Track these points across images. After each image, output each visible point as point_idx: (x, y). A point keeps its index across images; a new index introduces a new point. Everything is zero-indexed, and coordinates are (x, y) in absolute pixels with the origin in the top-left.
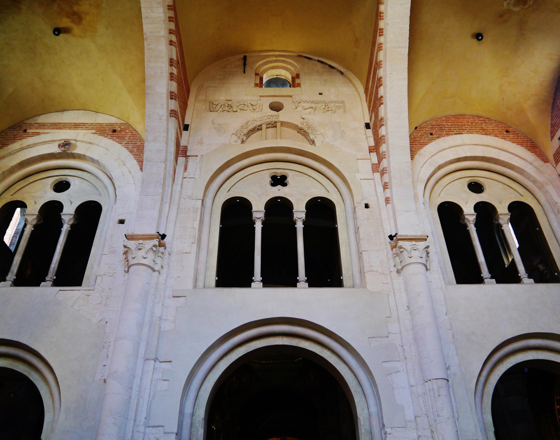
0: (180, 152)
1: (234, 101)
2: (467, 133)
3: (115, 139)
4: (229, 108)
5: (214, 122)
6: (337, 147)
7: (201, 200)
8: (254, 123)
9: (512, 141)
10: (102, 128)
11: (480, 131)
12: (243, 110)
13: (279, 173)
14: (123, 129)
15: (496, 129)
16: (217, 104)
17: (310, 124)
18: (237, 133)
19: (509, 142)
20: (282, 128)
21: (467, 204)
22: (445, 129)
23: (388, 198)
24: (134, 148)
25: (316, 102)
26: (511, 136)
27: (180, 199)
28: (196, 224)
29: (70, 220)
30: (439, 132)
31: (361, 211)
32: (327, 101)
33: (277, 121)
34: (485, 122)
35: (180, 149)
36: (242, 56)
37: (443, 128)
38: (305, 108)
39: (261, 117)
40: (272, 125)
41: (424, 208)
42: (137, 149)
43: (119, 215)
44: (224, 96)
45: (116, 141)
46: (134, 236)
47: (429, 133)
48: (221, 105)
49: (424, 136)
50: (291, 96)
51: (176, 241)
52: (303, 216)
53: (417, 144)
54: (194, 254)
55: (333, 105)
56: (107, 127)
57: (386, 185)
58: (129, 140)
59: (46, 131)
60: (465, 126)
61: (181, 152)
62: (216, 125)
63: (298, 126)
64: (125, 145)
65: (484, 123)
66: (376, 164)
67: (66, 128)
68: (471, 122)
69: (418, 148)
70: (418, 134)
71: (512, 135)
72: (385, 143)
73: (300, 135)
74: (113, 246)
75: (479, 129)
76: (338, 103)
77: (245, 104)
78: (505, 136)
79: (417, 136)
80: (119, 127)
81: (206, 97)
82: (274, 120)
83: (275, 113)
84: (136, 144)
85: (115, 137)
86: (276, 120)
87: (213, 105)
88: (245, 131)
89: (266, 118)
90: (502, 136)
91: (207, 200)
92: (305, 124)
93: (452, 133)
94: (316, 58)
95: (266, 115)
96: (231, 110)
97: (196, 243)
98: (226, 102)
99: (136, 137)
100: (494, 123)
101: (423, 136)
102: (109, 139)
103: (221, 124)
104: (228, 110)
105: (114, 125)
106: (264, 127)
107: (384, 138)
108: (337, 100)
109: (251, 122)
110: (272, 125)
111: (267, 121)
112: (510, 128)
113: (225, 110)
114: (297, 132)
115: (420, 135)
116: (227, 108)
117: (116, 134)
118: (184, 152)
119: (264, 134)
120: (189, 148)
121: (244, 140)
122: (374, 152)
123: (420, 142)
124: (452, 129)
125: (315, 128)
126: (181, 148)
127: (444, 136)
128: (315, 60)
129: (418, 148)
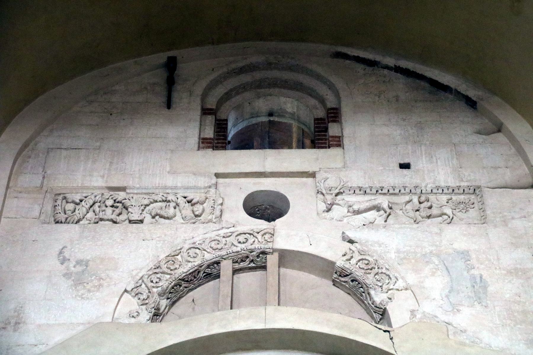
1: (131, 191)
4: (117, 211)
5: (67, 254)
6: (464, 331)
8: (194, 257)
12: (161, 217)
16: (78, 201)
17: (372, 257)
18: (140, 290)
20: (283, 270)
25: (391, 191)
32: (426, 187)
36: (162, 58)
38: (356, 207)
39: (217, 238)
40: (252, 261)
44: (103, 177)
48: (91, 202)
50: (313, 175)
55: (444, 198)
63: (332, 264)
73: (342, 292)
76: (460, 194)
77: (170, 198)
81: (44, 177)
82: (258, 245)
83: (261, 224)
86: (264, 246)
87: (67, 202)
88: (166, 282)
89: (232, 239)
92: (357, 257)
94: (390, 61)
95: (233, 233)
96: (123, 217)
98: (107, 194)
103: (88, 261)
104: (114, 217)
106: (226, 267)
108: (458, 185)
109: (185, 255)
110: (252, 261)
111: (235, 249)
113: (105, 217)
114: (332, 283)
116: (109, 210)
119: (227, 290)
121: (162, 309)
125: (387, 269)
128: (387, 67)
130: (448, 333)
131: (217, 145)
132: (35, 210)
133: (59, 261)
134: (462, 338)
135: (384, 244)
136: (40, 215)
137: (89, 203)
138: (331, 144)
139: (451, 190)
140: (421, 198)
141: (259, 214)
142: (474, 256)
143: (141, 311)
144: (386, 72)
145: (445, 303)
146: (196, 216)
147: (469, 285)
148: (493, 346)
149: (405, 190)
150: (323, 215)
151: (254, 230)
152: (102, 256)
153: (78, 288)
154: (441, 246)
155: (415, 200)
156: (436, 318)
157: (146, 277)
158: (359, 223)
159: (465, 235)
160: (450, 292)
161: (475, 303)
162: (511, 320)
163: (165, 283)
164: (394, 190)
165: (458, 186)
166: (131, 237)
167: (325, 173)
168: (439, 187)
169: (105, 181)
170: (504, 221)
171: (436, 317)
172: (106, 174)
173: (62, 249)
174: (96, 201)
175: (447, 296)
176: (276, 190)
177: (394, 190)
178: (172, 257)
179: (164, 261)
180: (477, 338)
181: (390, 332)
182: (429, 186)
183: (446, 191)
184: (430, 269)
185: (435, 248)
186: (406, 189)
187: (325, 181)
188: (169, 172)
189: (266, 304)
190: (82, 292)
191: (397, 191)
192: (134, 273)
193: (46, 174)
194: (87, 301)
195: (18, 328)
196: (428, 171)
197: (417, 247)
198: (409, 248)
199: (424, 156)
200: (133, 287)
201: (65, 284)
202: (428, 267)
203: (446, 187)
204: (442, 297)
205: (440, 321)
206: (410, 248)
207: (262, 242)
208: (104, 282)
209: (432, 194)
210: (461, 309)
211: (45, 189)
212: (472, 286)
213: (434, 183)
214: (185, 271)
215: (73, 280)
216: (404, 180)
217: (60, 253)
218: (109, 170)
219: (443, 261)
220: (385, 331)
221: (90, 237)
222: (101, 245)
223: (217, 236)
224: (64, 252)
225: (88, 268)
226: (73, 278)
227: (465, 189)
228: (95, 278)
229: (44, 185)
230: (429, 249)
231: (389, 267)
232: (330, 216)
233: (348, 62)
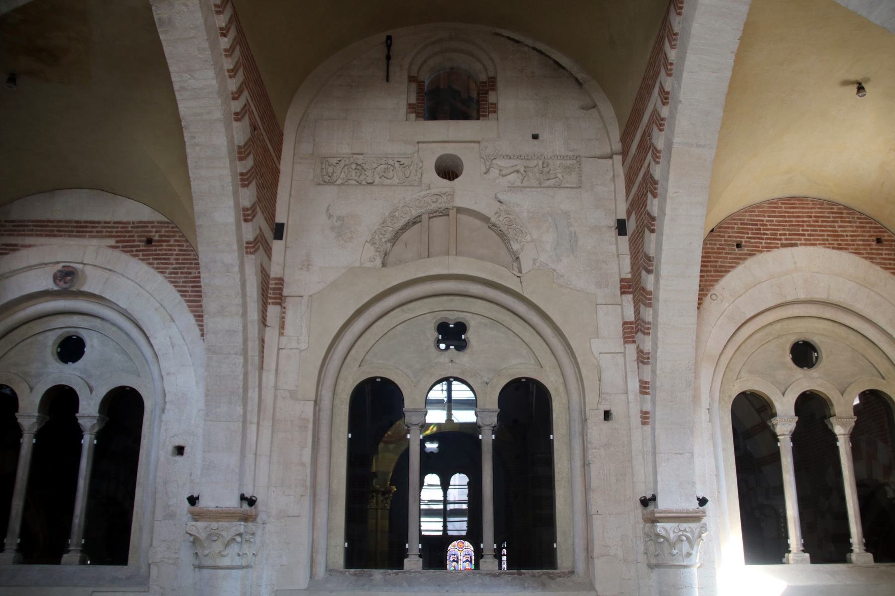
0: (270, 293)
1: (366, 156)
2: (805, 245)
3: (151, 261)
6: (562, 276)
7: (312, 403)
9: (885, 264)
10: (127, 234)
11: (830, 238)
13: (452, 318)
14: (165, 236)
15: (858, 236)
19: (878, 268)
20: (459, 216)
21: (783, 394)
22: (765, 234)
23: (647, 413)
24: (188, 285)
25: (526, 158)
26: (884, 252)
27: (275, 398)
28: (307, 453)
29: (93, 426)
30: (753, 241)
31: (597, 429)
32: (547, 155)
33: (450, 208)
34: (841, 217)
35: (270, 286)
37: (762, 232)
41: (708, 420)
42: (193, 287)
43: (173, 437)
45: (153, 267)
46: (202, 513)
47: (735, 244)
48: (343, 165)
49: (724, 251)
51: (274, 491)
52: (494, 420)
53: (710, 271)
54: (305, 521)
55: (558, 162)
56: (136, 232)
57: (645, 388)
58: (177, 263)
59: (29, 240)
60: (803, 226)
61: (272, 292)
62: (335, 220)
63: (489, 219)
64: (171, 277)
65: (839, 220)
66: (631, 323)
67: (62, 233)
68: (816, 217)
69: (711, 281)
70: (715, 244)
71: (886, 249)
72: (651, 307)
74: (169, 503)
75: (828, 235)
76: (567, 160)
78: (873, 254)
79: (713, 249)
80: (156, 232)
81: (314, 145)
82: (442, 203)
84: (190, 273)
85: (151, 257)
86: (447, 206)
90: (868, 254)
91: (323, 392)
93: (778, 244)
97: (308, 495)
99: (189, 257)
100: (858, 218)
101: (723, 249)
102: (140, 262)
105: (147, 227)
106: (425, 218)
107: (650, 297)
108: (567, 154)
112: (885, 232)
113: (351, 178)
115: (718, 246)
117: (153, 248)
118: (277, 294)
120: (286, 279)
122: (629, 293)
123: (716, 266)
124: (779, 232)
125: (522, 226)
126: (272, 284)
127: (761, 252)
129: (711, 281)
138: (491, 111)
139: (562, 158)
144: (526, 48)
146: (406, 178)
155: (540, 163)
164: (528, 157)
171: (547, 265)
175: (555, 249)
178: (392, 216)
188: (389, 141)
189: (449, 255)
214: (400, 225)
220: (518, 277)
233: (503, 39)
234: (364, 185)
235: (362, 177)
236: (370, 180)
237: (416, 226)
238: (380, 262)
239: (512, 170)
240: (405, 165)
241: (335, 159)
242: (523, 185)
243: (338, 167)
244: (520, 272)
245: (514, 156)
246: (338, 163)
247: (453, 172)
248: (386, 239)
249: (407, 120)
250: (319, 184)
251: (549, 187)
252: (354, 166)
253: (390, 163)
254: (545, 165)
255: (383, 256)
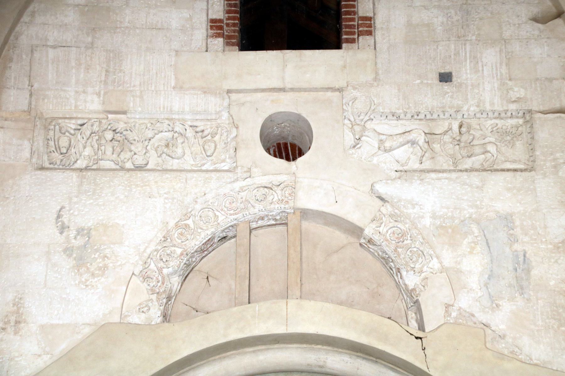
1: (133, 116)
6: (503, 337)
20: (305, 224)
25: (429, 117)
32: (468, 110)
44: (98, 94)
48: (88, 133)
62: (73, 233)
76: (507, 118)
81: (31, 95)
130: (485, 338)
131: (228, 22)
132: (25, 148)
133: (58, 230)
134: (501, 346)
135: (418, 205)
136: (31, 156)
137: (86, 136)
138: (361, 31)
140: (462, 129)
141: (277, 131)
142: (518, 223)
143: (151, 304)
145: (483, 296)
147: (511, 268)
148: (533, 358)
149: (444, 115)
150: (351, 152)
151: (273, 183)
152: (104, 222)
153: (81, 271)
154: (482, 207)
155: (455, 127)
156: (472, 318)
157: (155, 253)
158: (391, 165)
159: (509, 189)
160: (489, 279)
161: (516, 295)
162: (555, 319)
163: (176, 262)
164: (432, 115)
165: (505, 110)
166: (135, 192)
167: (354, 90)
168: (483, 111)
169: (101, 102)
170: (555, 167)
171: (473, 315)
172: (102, 90)
173: (60, 211)
174: (93, 132)
176: (296, 112)
177: (432, 115)
179: (174, 230)
180: (517, 346)
181: (422, 339)
182: (472, 109)
183: (491, 114)
184: (469, 243)
185: (476, 211)
186: (446, 114)
187: (353, 103)
188: (174, 88)
190: (86, 276)
191: (435, 116)
192: (142, 248)
193: (33, 88)
194: (92, 291)
195: (19, 329)
196: (472, 85)
197: (455, 208)
198: (445, 210)
199: (468, 61)
200: (141, 269)
201: (66, 263)
202: (466, 240)
203: (492, 111)
204: (480, 286)
205: (477, 322)
206: (447, 210)
207: (283, 200)
208: (109, 261)
209: (475, 119)
210: (501, 303)
211: (33, 113)
212: (514, 269)
213: (478, 106)
214: (197, 243)
215: (75, 259)
216: (444, 101)
217: (58, 217)
218: (106, 83)
219: (483, 231)
220: (417, 338)
221: (90, 192)
222: (104, 205)
223: (231, 190)
224: (63, 215)
225: (91, 240)
226: (75, 255)
227: (513, 114)
228: (99, 255)
229: (33, 107)
230: (469, 212)
231: (423, 241)
232: (358, 154)
234: (129, 170)
235: (126, 155)
236: (139, 160)
237: (227, 244)
238: (159, 313)
239: (401, 140)
240: (206, 133)
241: (73, 121)
242: (423, 167)
243: (79, 137)
244: (421, 328)
245: (405, 114)
246: (79, 130)
247: (293, 146)
248: (171, 270)
249: (207, 51)
250: (42, 168)
251: (472, 170)
252: (109, 135)
253: (177, 129)
254: (464, 130)
255: (165, 301)
